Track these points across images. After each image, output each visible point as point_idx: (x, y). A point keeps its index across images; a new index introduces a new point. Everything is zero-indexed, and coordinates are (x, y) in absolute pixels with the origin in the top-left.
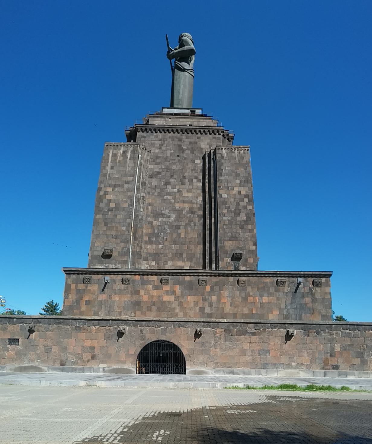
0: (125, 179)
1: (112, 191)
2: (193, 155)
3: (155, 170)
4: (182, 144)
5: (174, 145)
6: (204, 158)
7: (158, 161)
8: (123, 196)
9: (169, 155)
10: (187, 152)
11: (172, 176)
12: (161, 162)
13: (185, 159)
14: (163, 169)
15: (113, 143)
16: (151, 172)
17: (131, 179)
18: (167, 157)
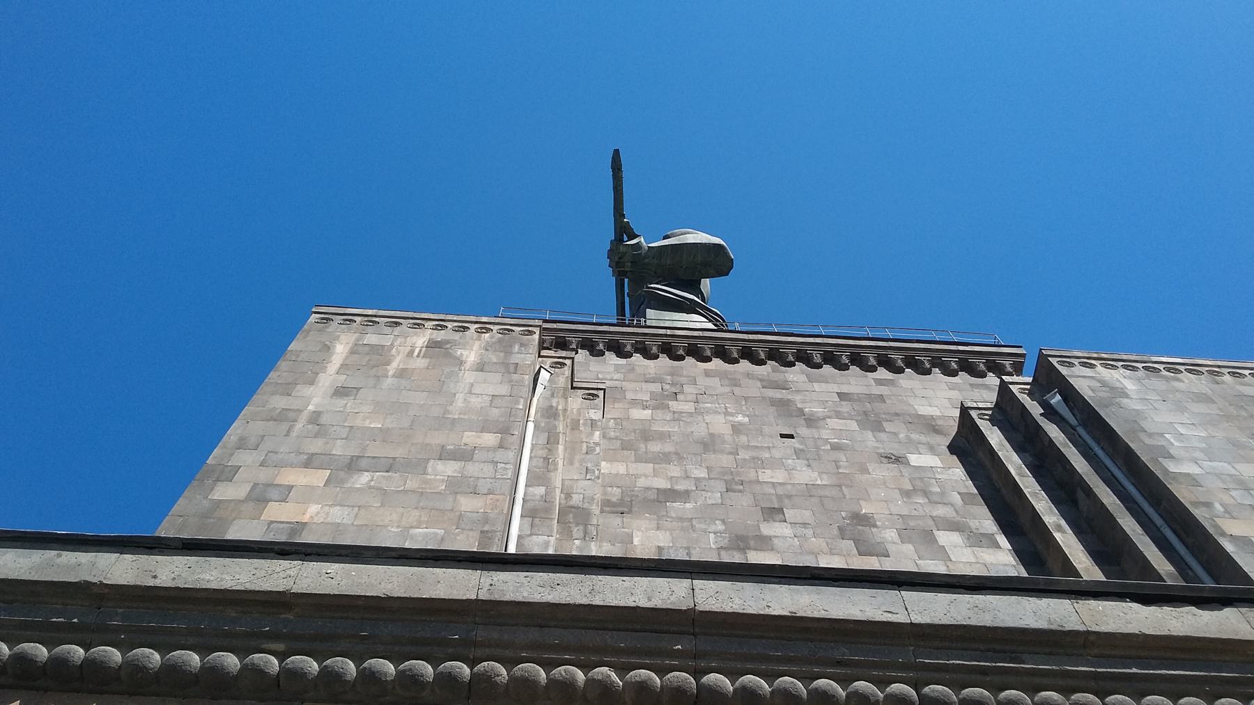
0: (437, 439)
1: (322, 485)
2: (883, 436)
3: (642, 483)
4: (798, 398)
5: (746, 399)
6: (967, 445)
7: (655, 447)
8: (416, 513)
9: (726, 430)
10: (834, 423)
11: (774, 513)
12: (677, 454)
13: (836, 447)
14: (698, 480)
15: (370, 312)
16: (617, 491)
17: (490, 439)
18: (712, 435)
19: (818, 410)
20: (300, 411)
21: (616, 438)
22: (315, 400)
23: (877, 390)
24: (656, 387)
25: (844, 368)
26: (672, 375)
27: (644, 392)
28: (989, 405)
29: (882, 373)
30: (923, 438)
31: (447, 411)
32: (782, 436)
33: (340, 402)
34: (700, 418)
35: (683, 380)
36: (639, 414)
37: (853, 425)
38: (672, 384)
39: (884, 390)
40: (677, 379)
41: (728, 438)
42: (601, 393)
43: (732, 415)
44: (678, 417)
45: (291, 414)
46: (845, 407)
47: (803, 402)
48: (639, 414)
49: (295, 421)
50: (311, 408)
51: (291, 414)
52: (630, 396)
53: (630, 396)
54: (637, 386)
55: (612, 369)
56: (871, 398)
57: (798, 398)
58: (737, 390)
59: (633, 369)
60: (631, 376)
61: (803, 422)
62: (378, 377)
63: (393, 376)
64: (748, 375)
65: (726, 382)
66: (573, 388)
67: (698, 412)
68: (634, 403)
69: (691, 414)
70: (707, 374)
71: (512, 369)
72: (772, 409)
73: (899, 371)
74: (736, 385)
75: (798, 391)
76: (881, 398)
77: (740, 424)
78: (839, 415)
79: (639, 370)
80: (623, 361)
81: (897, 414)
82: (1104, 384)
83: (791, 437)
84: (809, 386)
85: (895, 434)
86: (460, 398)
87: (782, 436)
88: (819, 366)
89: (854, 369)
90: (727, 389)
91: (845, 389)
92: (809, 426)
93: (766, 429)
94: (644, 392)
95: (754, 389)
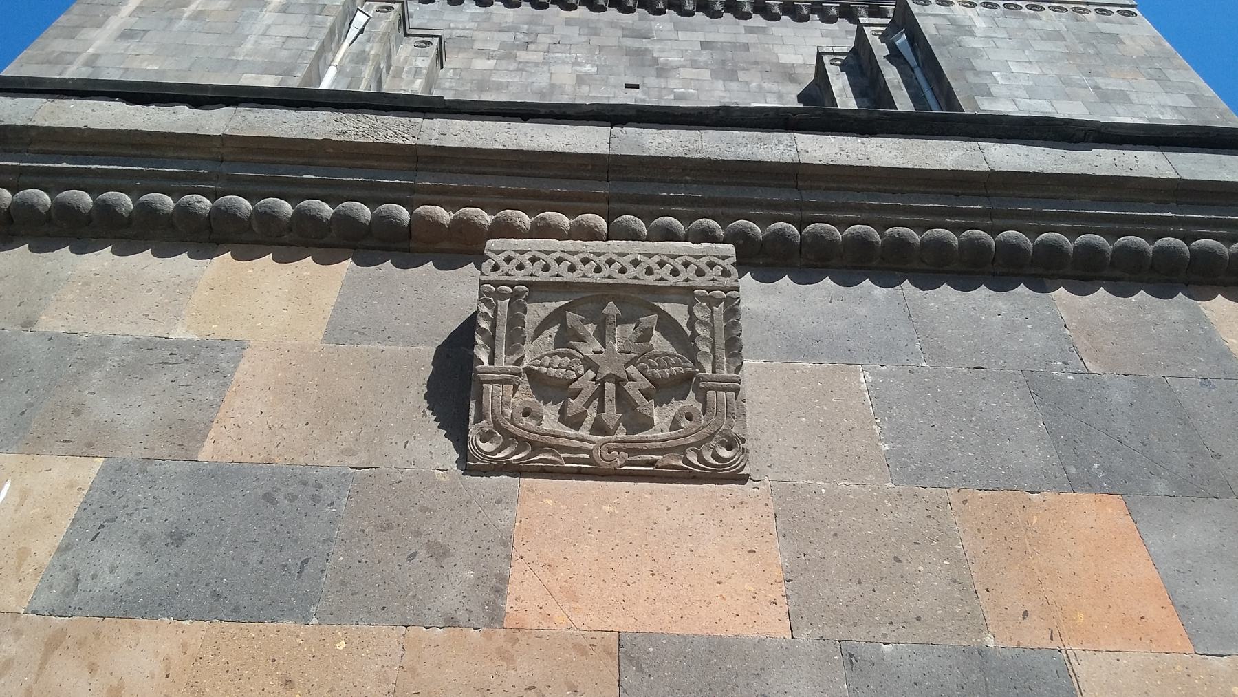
2: (734, 85)
5: (601, 48)
10: (688, 73)
19: (674, 59)
20: (78, 54)
21: (450, 89)
22: (98, 43)
23: (744, 38)
24: (508, 37)
25: (715, 15)
26: (529, 23)
27: (492, 41)
28: (846, 50)
29: (758, 20)
30: (775, 87)
31: (233, 54)
32: (627, 86)
33: (123, 45)
34: (546, 68)
35: (540, 29)
36: (481, 64)
37: (707, 74)
38: (526, 34)
39: (752, 38)
40: (534, 27)
41: (568, 89)
42: (436, 41)
43: (580, 64)
44: (522, 67)
45: (69, 57)
46: (705, 56)
47: (661, 51)
48: (481, 64)
49: (71, 63)
50: (91, 50)
51: (69, 57)
52: (477, 46)
53: (477, 46)
54: (488, 35)
55: (467, 18)
56: (735, 46)
57: (657, 47)
58: (594, 40)
59: (490, 18)
60: (485, 25)
61: (653, 72)
62: (171, 20)
63: (189, 18)
64: (612, 24)
65: (586, 31)
66: (406, 35)
67: (546, 62)
68: (482, 53)
69: (537, 64)
70: (568, 23)
71: (318, 10)
72: (625, 59)
73: (776, 18)
74: (595, 35)
75: (660, 40)
76: (746, 47)
77: (587, 74)
78: (694, 64)
79: (495, 19)
80: (481, 10)
81: (756, 63)
82: (953, 22)
83: (637, 87)
84: (673, 35)
85: (747, 83)
86: (252, 39)
87: (627, 86)
88: (690, 14)
89: (728, 17)
90: (584, 39)
91: (710, 37)
92: (658, 76)
93: (612, 79)
94: (492, 41)
95: (612, 38)
